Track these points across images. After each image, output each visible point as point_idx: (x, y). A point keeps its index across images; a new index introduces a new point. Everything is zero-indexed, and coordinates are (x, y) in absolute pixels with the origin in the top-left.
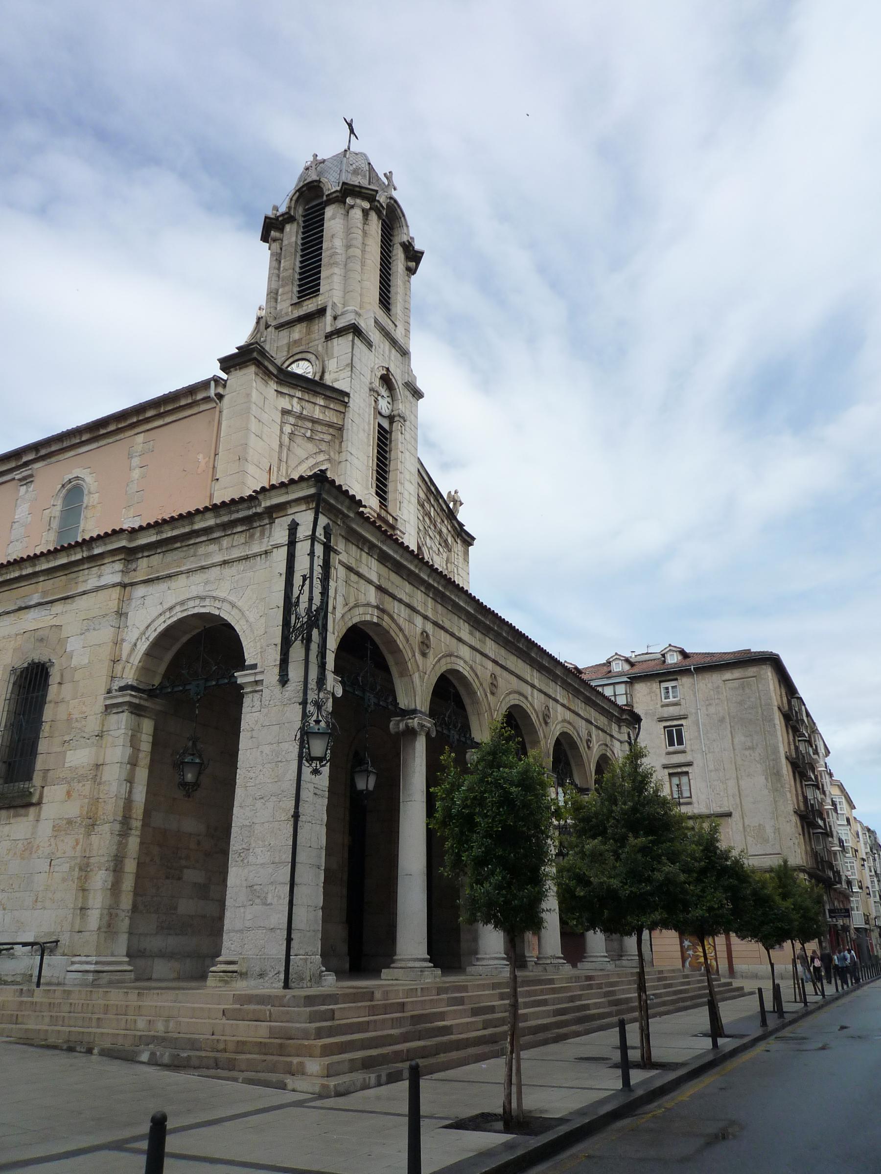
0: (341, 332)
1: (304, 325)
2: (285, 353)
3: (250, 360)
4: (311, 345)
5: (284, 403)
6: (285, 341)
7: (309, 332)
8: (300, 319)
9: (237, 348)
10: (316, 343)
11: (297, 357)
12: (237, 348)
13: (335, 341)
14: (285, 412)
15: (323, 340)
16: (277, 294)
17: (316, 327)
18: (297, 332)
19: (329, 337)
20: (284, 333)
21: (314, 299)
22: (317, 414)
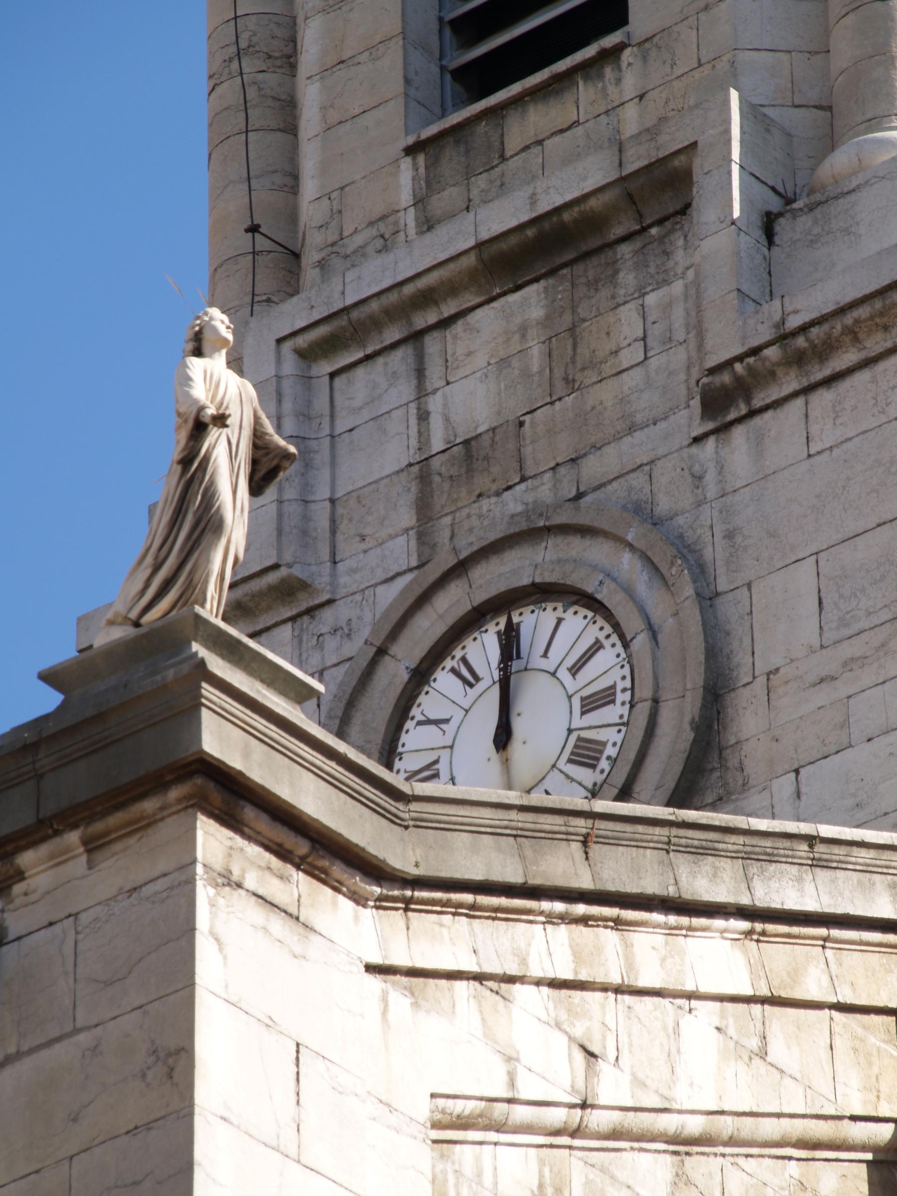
0: (824, 351)
1: (530, 302)
2: (401, 551)
3: (155, 783)
4: (594, 468)
5: (455, 1048)
6: (395, 452)
7: (570, 365)
8: (507, 264)
9: (50, 677)
10: (636, 448)
11: (492, 578)
12: (50, 677)
13: (783, 429)
14: (455, 1124)
15: (689, 419)
16: (288, 61)
17: (628, 320)
18: (480, 372)
19: (727, 399)
20: (376, 389)
21: (585, 92)
22: (698, 1067)
